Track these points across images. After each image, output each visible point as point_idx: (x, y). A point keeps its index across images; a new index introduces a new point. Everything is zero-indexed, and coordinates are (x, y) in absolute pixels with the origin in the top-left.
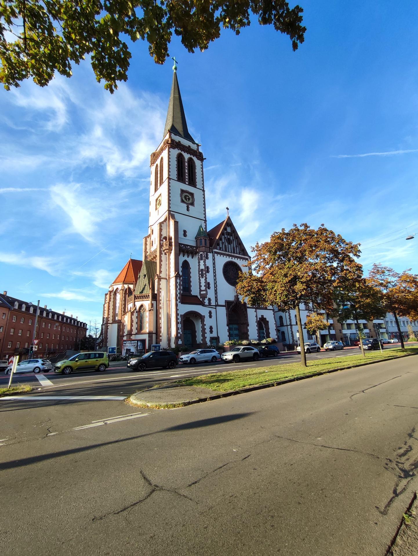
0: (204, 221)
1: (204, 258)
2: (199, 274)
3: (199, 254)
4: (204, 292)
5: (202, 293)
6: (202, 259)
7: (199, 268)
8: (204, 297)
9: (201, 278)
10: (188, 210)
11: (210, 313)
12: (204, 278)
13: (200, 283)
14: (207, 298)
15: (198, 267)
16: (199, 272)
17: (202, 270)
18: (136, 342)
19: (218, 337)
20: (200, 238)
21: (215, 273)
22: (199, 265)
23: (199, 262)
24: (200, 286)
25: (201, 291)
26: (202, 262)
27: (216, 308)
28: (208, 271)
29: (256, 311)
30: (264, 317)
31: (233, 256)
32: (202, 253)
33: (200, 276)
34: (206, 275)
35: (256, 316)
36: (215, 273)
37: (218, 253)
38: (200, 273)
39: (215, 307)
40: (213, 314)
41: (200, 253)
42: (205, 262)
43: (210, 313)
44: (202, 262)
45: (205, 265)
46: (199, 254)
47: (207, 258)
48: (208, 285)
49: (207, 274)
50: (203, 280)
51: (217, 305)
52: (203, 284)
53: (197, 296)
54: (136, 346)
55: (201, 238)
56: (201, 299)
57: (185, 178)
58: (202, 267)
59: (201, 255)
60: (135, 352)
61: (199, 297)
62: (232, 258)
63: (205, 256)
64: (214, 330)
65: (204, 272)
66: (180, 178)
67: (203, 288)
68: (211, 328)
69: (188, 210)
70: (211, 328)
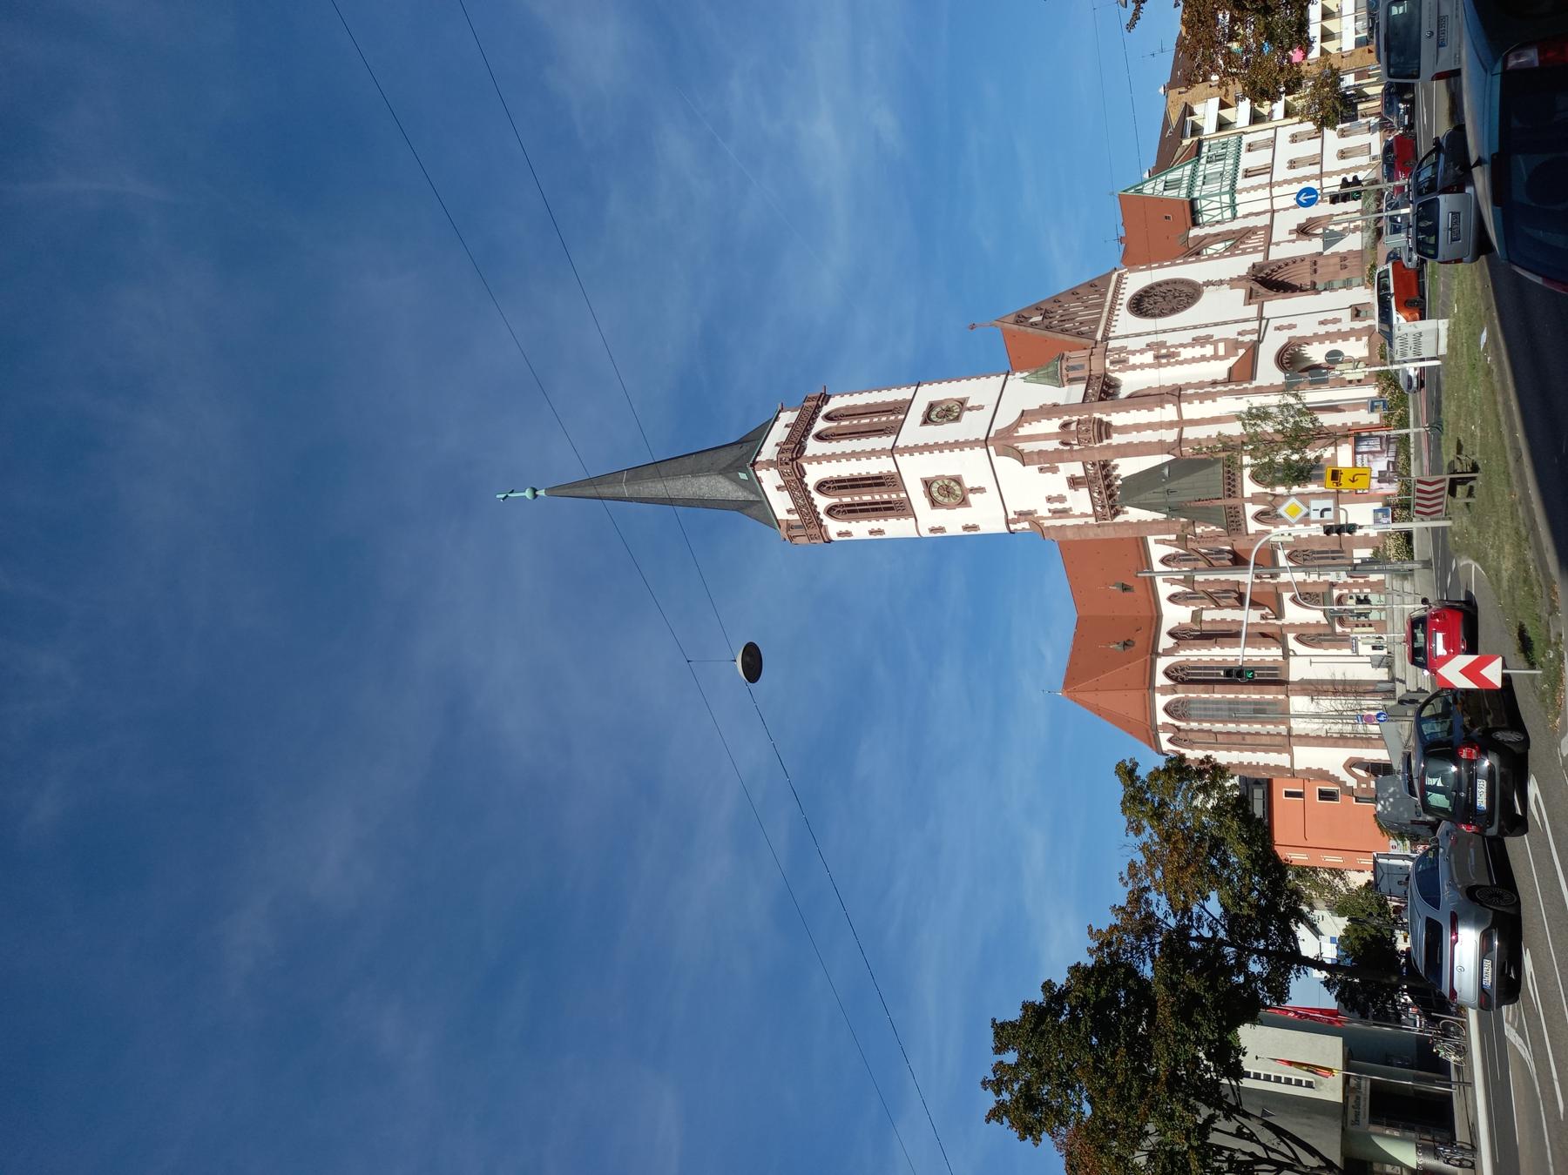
0: (1009, 377)
1: (1122, 355)
2: (1168, 364)
3: (1112, 368)
4: (1221, 347)
5: (1221, 352)
6: (1124, 361)
7: (1150, 366)
8: (1233, 345)
9: (1180, 359)
10: (980, 408)
11: (1278, 328)
12: (1180, 349)
13: (1194, 360)
14: (1237, 339)
15: (1147, 369)
16: (1160, 365)
17: (1157, 357)
18: (1359, 457)
19: (1351, 306)
20: (1064, 372)
21: (1165, 331)
22: (1142, 366)
23: (1134, 367)
24: (1203, 358)
25: (1215, 357)
26: (1133, 360)
27: (1268, 319)
28: (1162, 344)
29: (1278, 244)
30: (1295, 227)
31: (1113, 302)
32: (1108, 361)
33: (1174, 360)
34: (1172, 346)
35: (1293, 241)
36: (1165, 331)
37: (1106, 330)
38: (1164, 361)
39: (1264, 322)
40: (1285, 322)
41: (1108, 365)
42: (1133, 353)
43: (1278, 328)
44: (1133, 360)
45: (1142, 352)
46: (1112, 368)
47: (1122, 349)
48: (1198, 341)
49: (1168, 344)
50: (1186, 353)
51: (1260, 318)
52: (1197, 352)
53: (1230, 370)
54: (1371, 457)
55: (1064, 367)
56: (1241, 352)
57: (896, 421)
58: (1148, 357)
59: (1112, 363)
60: (1387, 459)
61: (1232, 361)
62: (1121, 304)
63: (1116, 354)
64: (1329, 316)
65: (1164, 351)
66: (894, 429)
67: (1209, 350)
68: (1322, 323)
69: (980, 408)
70: (1322, 323)
